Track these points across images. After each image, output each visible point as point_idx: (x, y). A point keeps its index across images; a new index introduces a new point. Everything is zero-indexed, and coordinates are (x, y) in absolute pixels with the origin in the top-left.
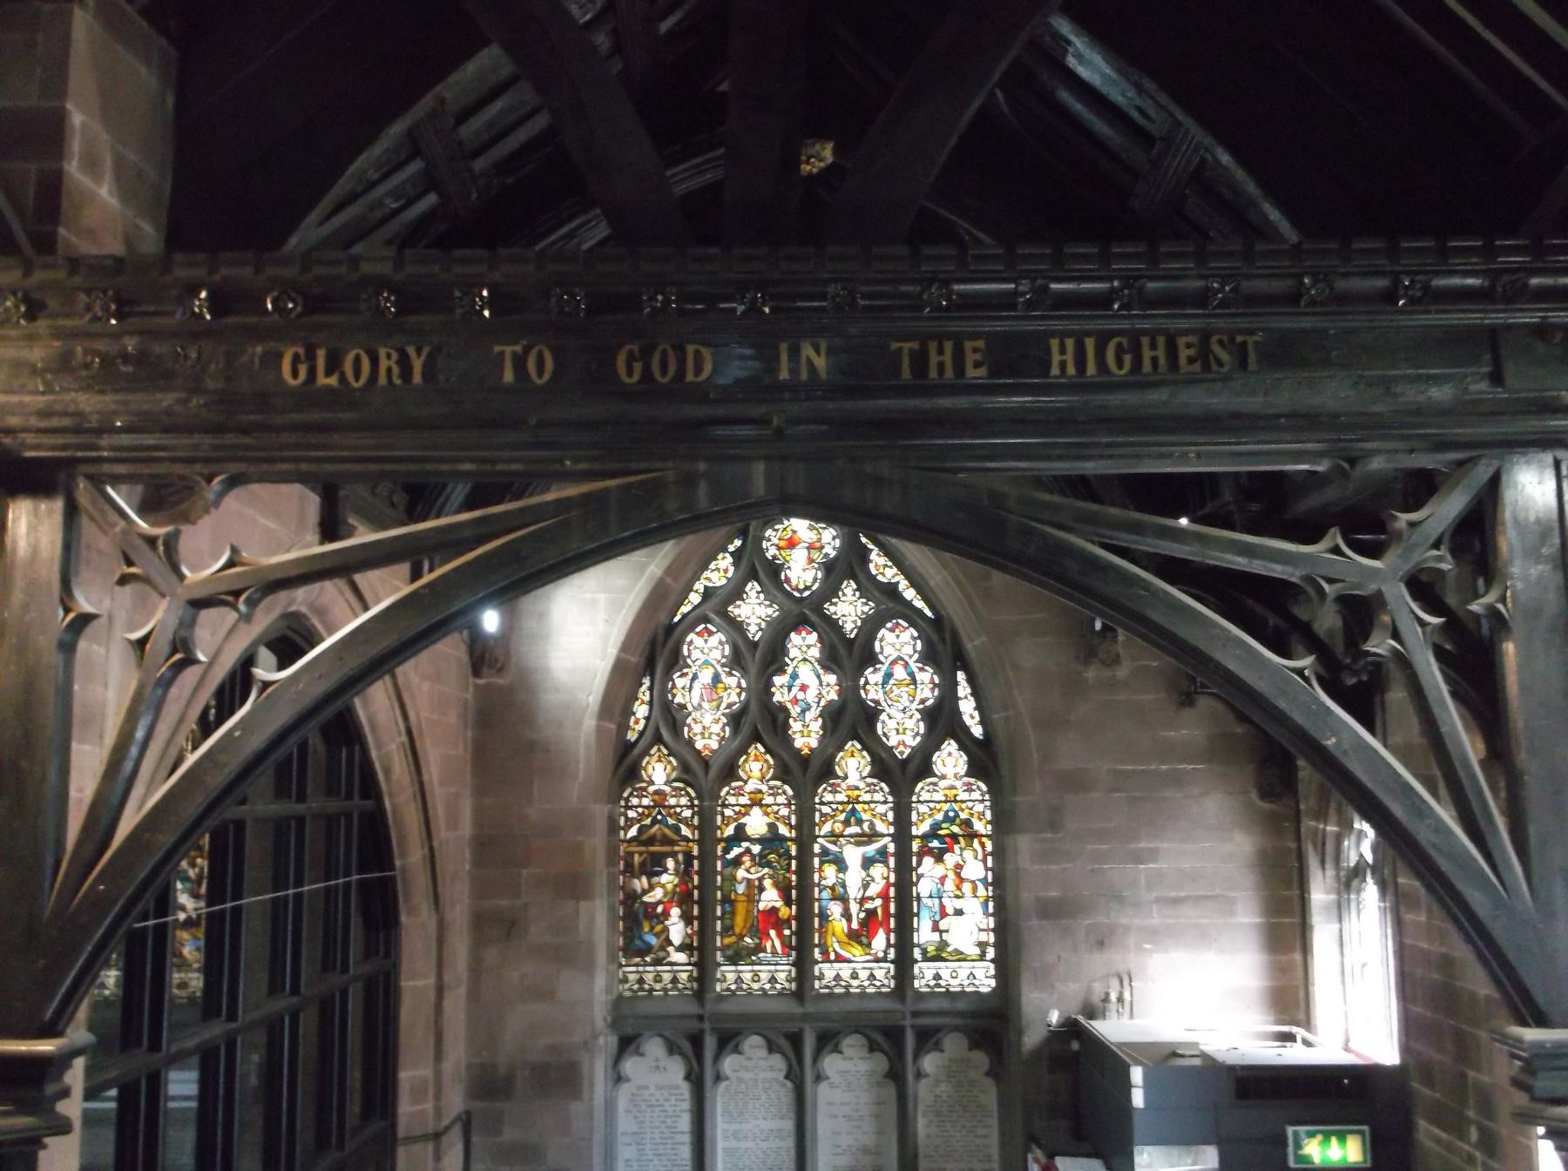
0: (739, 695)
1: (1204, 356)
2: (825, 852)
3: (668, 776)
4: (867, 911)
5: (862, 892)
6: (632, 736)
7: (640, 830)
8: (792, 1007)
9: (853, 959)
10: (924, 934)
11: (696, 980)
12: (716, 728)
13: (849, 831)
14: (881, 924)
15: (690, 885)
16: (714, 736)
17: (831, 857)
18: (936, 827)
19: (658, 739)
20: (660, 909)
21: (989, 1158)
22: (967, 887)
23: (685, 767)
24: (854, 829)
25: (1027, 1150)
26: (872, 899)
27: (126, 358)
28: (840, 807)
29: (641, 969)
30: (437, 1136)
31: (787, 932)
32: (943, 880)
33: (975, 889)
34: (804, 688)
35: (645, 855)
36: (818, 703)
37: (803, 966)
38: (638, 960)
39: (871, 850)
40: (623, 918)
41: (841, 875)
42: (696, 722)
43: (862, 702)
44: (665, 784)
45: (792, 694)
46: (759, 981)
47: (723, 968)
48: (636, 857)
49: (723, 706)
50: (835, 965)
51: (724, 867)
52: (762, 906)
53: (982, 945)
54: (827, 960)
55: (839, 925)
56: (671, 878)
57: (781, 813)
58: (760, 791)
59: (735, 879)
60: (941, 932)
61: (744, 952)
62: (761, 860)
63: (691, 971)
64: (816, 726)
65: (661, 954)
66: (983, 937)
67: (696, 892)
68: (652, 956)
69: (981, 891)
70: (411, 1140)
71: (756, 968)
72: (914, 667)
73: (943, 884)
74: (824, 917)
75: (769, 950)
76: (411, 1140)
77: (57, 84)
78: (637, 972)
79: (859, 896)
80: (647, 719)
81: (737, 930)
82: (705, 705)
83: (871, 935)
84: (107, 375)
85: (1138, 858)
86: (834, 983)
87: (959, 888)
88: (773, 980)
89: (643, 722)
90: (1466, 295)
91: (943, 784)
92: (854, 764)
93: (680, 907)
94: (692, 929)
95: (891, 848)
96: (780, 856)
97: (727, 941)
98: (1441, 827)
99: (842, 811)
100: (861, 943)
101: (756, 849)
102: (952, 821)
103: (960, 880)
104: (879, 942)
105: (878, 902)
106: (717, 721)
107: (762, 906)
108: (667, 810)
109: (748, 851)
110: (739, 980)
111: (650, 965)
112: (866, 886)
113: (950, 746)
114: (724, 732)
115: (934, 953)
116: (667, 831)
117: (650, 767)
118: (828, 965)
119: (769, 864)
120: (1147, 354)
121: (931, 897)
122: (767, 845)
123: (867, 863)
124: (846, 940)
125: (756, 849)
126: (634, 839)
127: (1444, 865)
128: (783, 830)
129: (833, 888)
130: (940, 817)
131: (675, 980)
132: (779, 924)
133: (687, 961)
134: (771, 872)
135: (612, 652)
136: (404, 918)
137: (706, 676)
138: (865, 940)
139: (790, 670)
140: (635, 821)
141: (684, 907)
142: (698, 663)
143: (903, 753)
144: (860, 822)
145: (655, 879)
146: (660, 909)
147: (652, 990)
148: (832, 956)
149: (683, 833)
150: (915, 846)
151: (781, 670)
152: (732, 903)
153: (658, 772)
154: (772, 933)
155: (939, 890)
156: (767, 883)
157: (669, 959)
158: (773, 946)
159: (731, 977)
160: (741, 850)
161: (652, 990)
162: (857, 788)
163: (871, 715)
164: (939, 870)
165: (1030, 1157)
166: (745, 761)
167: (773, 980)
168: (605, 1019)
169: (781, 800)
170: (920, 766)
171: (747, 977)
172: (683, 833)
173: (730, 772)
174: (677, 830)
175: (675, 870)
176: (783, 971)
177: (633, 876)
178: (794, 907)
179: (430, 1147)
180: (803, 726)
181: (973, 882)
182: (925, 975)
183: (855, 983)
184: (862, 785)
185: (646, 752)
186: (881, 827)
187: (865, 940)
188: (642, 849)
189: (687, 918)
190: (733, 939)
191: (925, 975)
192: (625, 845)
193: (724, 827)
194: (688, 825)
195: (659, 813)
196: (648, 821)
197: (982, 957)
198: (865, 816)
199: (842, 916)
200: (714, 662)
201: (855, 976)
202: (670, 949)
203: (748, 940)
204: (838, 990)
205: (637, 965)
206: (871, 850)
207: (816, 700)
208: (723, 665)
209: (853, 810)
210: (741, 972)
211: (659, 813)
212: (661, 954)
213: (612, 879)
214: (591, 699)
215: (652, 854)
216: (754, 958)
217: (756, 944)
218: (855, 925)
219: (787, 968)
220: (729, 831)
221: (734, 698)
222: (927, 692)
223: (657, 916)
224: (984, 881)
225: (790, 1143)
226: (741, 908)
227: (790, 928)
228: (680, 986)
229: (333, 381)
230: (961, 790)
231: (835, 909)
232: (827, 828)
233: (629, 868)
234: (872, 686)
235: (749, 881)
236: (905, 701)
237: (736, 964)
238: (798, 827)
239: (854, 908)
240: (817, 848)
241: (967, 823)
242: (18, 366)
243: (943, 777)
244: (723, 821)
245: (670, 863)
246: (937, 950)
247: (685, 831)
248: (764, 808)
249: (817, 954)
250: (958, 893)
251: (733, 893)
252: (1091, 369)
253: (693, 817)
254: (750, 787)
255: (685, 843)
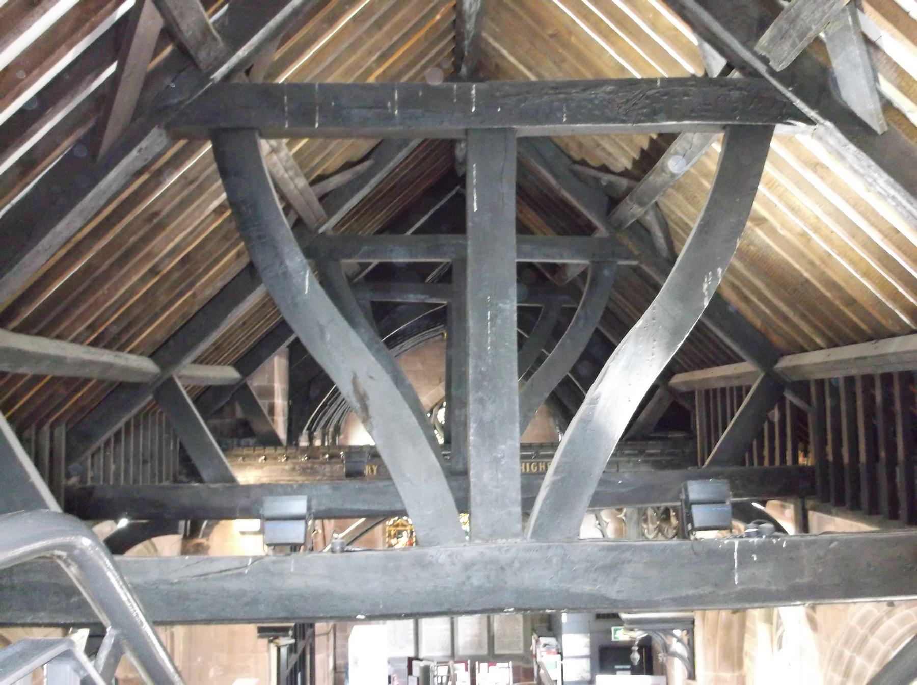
21: (519, 637)
25: (532, 634)
27: (308, 468)
30: (328, 633)
70: (320, 635)
76: (320, 635)
77: (271, 380)
84: (304, 471)
120: (540, 467)
126: (390, 526)
145: (399, 539)
165: (533, 637)
177: (391, 538)
179: (325, 637)
188: (394, 528)
213: (384, 540)
225: (449, 633)
233: (390, 535)
242: (284, 470)
245: (405, 533)
252: (528, 470)
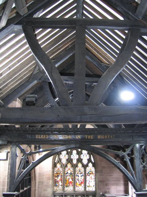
1: (110, 137)
2: (77, 175)
6: (56, 162)
8: (73, 192)
10: (87, 184)
18: (89, 172)
19: (59, 162)
23: (62, 165)
24: (80, 172)
37: (74, 188)
39: (82, 175)
43: (81, 158)
53: (94, 186)
54: (77, 187)
55: (78, 183)
62: (70, 176)
69: (94, 180)
72: (87, 154)
74: (76, 182)
83: (81, 184)
85: (111, 176)
88: (71, 189)
90: (131, 133)
92: (80, 165)
95: (84, 175)
98: (130, 175)
104: (83, 185)
110: (67, 189)
112: (81, 179)
113: (90, 163)
123: (81, 176)
127: (130, 178)
128: (72, 172)
130: (89, 171)
131: (60, 189)
132: (71, 183)
136: (32, 182)
137: (64, 155)
143: (85, 164)
144: (80, 172)
150: (87, 174)
151: (72, 154)
153: (58, 166)
156: (70, 178)
159: (66, 189)
163: (82, 160)
167: (71, 189)
169: (72, 169)
170: (87, 165)
171: (68, 189)
173: (66, 166)
182: (87, 189)
185: (57, 163)
186: (83, 172)
189: (62, 182)
191: (87, 189)
198: (81, 171)
201: (80, 189)
206: (82, 175)
220: (66, 172)
222: (88, 157)
226: (67, 181)
229: (40, 138)
231: (78, 181)
233: (55, 176)
234: (82, 156)
238: (74, 172)
239: (80, 181)
240: (76, 175)
241: (92, 172)
245: (60, 176)
247: (61, 172)
249: (76, 186)
252: (101, 138)
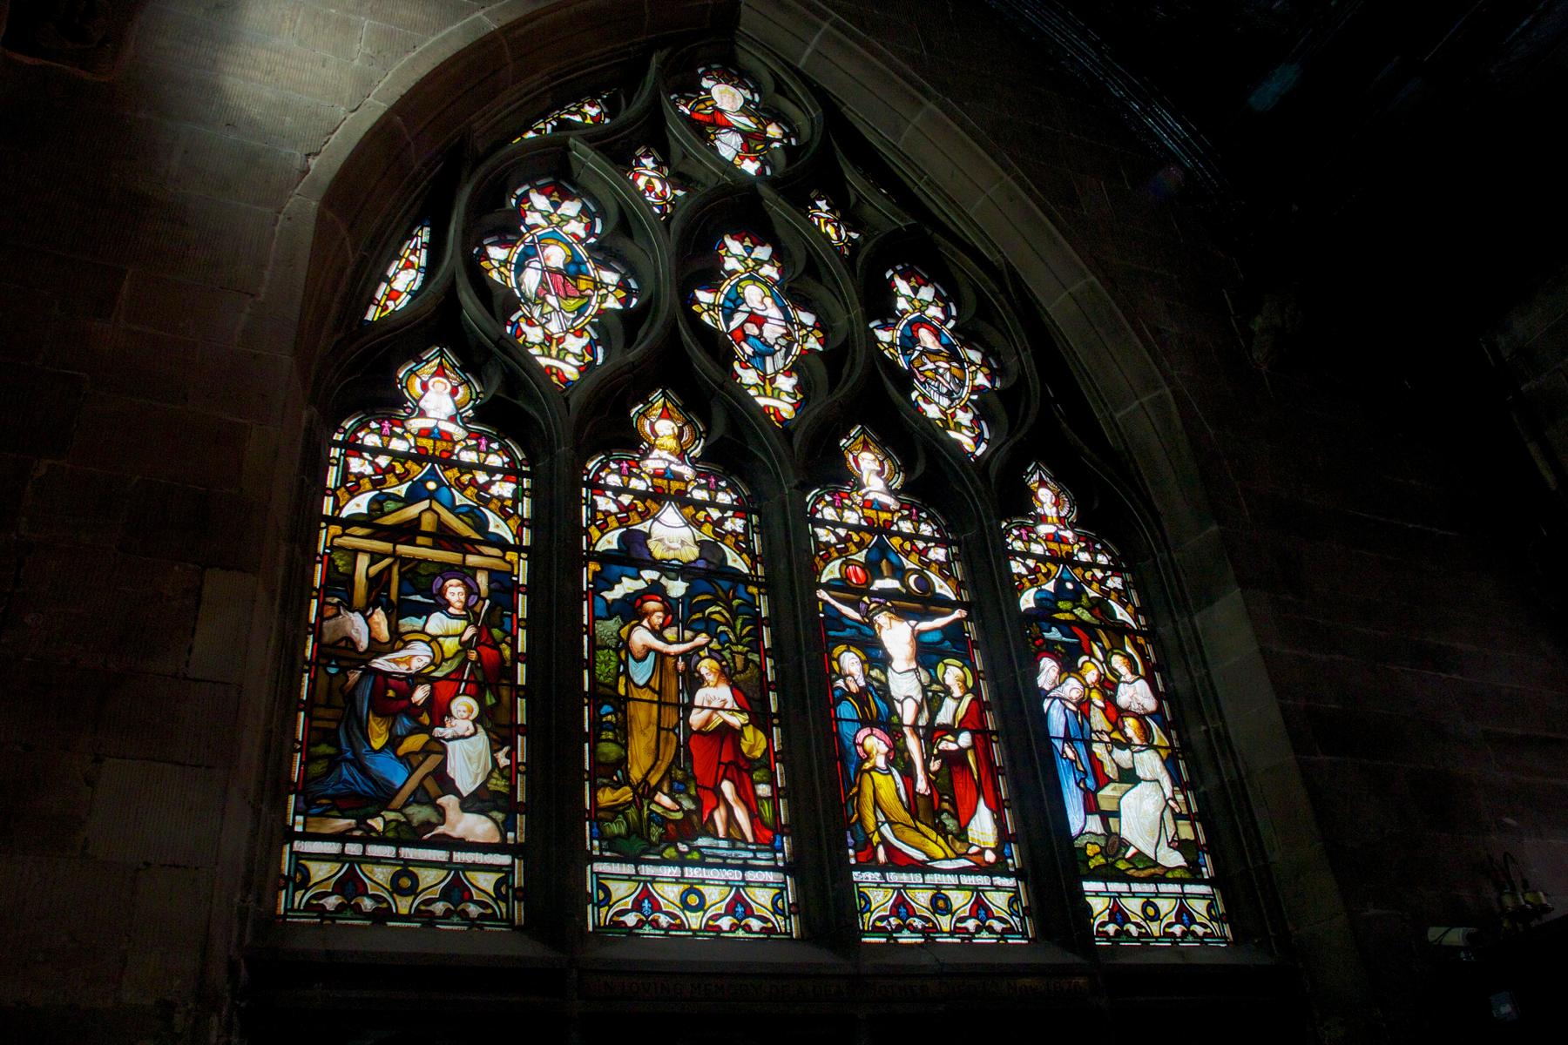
0: (624, 301)
3: (458, 407)
4: (944, 755)
5: (926, 714)
7: (377, 506)
9: (937, 865)
11: (522, 895)
12: (575, 344)
13: (879, 584)
14: (980, 790)
15: (507, 653)
16: (570, 358)
17: (848, 633)
20: (420, 694)
22: (1131, 726)
24: (891, 584)
26: (951, 730)
28: (856, 538)
29: (353, 849)
31: (763, 790)
32: (1084, 705)
33: (1146, 732)
34: (759, 321)
35: (387, 561)
36: (789, 347)
38: (342, 824)
40: (310, 706)
41: (875, 673)
42: (530, 323)
44: (452, 419)
45: (734, 325)
46: (701, 907)
47: (600, 867)
48: (363, 561)
49: (591, 311)
50: (893, 877)
51: (594, 618)
52: (696, 719)
54: (869, 864)
55: (888, 786)
56: (458, 625)
57: (728, 526)
58: (679, 477)
59: (629, 651)
60: (1105, 816)
61: (656, 832)
63: (508, 871)
64: (786, 383)
65: (420, 813)
66: (1186, 832)
67: (521, 669)
68: (391, 815)
69: (1158, 737)
71: (692, 872)
73: (1087, 717)
75: (721, 833)
78: (339, 858)
79: (922, 722)
80: (414, 295)
81: (636, 774)
82: (552, 300)
86: (894, 921)
87: (1117, 726)
88: (739, 906)
89: (404, 300)
91: (1043, 529)
93: (479, 699)
94: (508, 756)
96: (734, 613)
97: (606, 797)
99: (860, 545)
100: (941, 830)
101: (677, 588)
102: (1076, 596)
103: (1116, 714)
104: (983, 827)
105: (965, 739)
106: (579, 333)
107: (696, 719)
108: (452, 474)
109: (656, 590)
110: (645, 899)
111: (382, 840)
114: (593, 353)
115: (1103, 861)
116: (447, 516)
117: (417, 383)
118: (874, 876)
119: (709, 626)
121: (1067, 738)
122: (704, 585)
123: (927, 654)
124: (905, 816)
125: (677, 588)
129: (861, 697)
130: (1050, 587)
131: (456, 890)
133: (497, 839)
134: (715, 645)
135: (377, 106)
137: (556, 256)
138: (951, 824)
139: (726, 287)
140: (366, 483)
141: (490, 700)
142: (539, 232)
145: (409, 623)
146: (420, 694)
147: (383, 914)
148: (881, 855)
149: (492, 529)
152: (621, 703)
154: (727, 788)
155: (1082, 727)
156: (706, 667)
157: (440, 830)
158: (731, 819)
159: (623, 892)
160: (641, 585)
161: (383, 914)
162: (884, 508)
164: (1072, 688)
166: (644, 415)
168: (232, 968)
171: (669, 894)
172: (492, 529)
174: (481, 524)
175: (466, 607)
176: (764, 885)
178: (776, 731)
180: (763, 378)
181: (1140, 718)
183: (945, 922)
184: (888, 500)
187: (951, 824)
190: (625, 794)
192: (335, 529)
193: (595, 533)
194: (506, 517)
195: (432, 475)
196: (402, 490)
197: (1192, 873)
198: (908, 565)
199: (889, 761)
200: (570, 239)
201: (940, 903)
202: (450, 802)
203: (666, 801)
204: (906, 938)
205: (342, 837)
207: (783, 342)
208: (589, 248)
209: (882, 550)
210: (654, 880)
211: (432, 475)
212: (420, 813)
214: (313, 162)
215: (403, 560)
216: (683, 848)
217: (687, 813)
218: (922, 786)
219: (769, 876)
220: (609, 541)
221: (612, 303)
223: (413, 711)
224: (1157, 714)
226: (642, 715)
227: (772, 781)
228: (473, 910)
230: (1076, 547)
231: (876, 745)
232: (831, 572)
235: (661, 656)
236: (946, 382)
237: (637, 861)
238: (767, 559)
239: (913, 745)
243: (1043, 519)
244: (593, 519)
245: (455, 592)
246: (1104, 852)
247: (497, 526)
248: (690, 510)
250: (1116, 735)
251: (622, 680)
253: (516, 499)
254: (651, 465)
255: (496, 552)
